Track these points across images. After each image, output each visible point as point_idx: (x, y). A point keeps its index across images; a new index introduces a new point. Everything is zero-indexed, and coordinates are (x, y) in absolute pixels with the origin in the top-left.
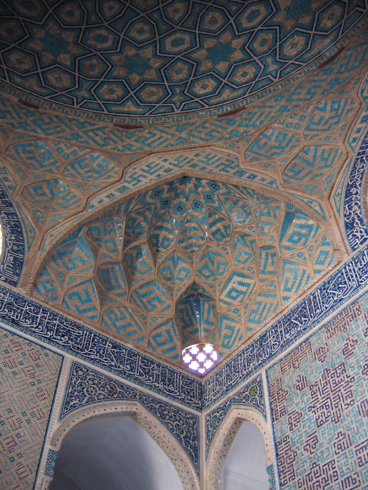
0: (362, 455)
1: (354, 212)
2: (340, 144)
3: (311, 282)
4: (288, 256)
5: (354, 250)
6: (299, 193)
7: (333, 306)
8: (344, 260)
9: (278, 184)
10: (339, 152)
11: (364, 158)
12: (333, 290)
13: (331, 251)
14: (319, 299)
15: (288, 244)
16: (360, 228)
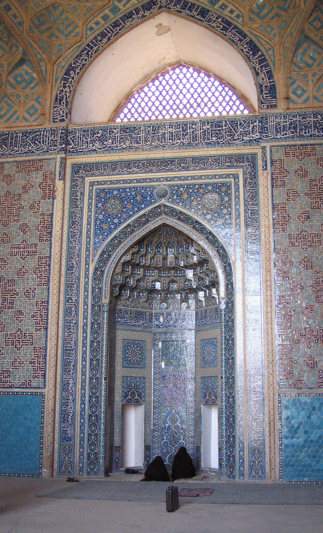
0: (13, 250)
1: (66, 92)
2: (80, 23)
3: (18, 124)
4: (9, 92)
5: (54, 122)
6: (36, 46)
7: (26, 153)
8: (46, 125)
9: (25, 28)
10: (77, 30)
11: (90, 53)
12: (30, 141)
13: (39, 111)
14: (19, 140)
15: (12, 81)
16: (64, 109)
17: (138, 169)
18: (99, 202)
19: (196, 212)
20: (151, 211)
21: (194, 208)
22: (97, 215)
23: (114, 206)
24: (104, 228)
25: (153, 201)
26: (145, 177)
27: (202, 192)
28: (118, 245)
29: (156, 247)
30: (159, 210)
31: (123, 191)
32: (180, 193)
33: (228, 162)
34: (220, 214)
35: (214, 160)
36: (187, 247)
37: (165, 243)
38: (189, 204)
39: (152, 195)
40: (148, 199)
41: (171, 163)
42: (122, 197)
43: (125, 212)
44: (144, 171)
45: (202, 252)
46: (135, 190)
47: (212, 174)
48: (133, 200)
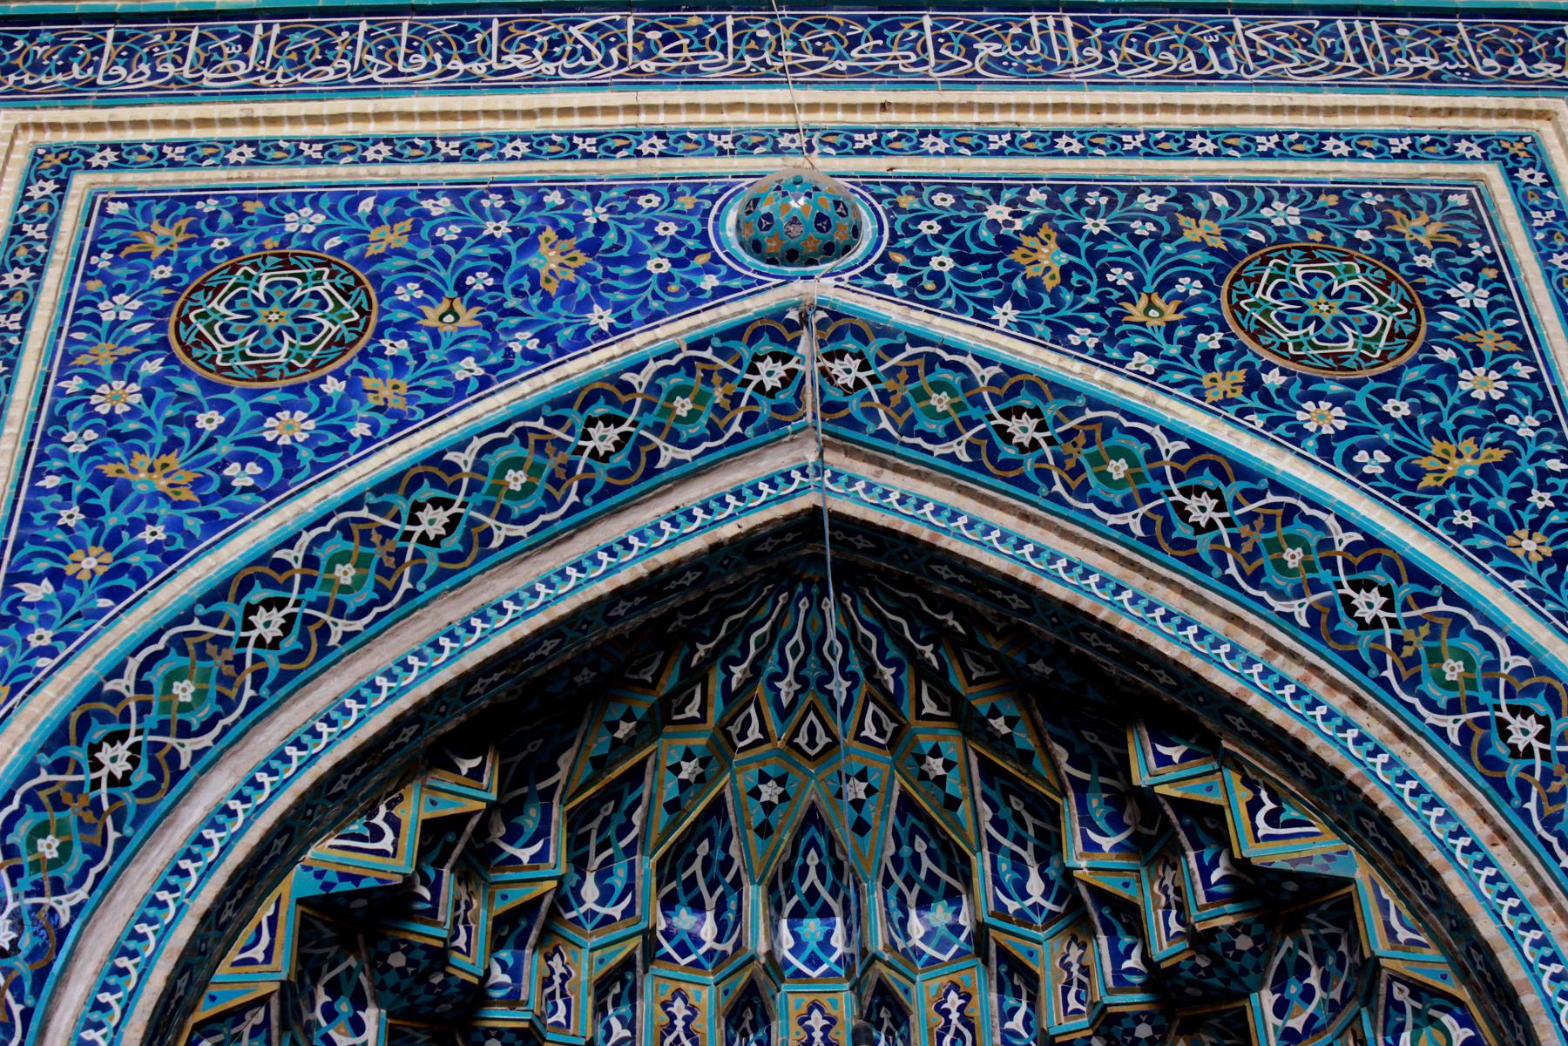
17: (549, 57)
18: (121, 289)
19: (1178, 377)
20: (684, 366)
21: (1152, 351)
22: (74, 385)
23: (274, 317)
24: (143, 482)
25: (709, 282)
26: (621, 121)
27: (1218, 243)
28: (284, 677)
29: (667, 869)
30: (771, 373)
31: (386, 210)
32: (985, 234)
33: (1420, 51)
34: (1434, 399)
35: (1285, 35)
36: (1008, 877)
37: (764, 830)
38: (1092, 317)
39: (691, 243)
40: (657, 264)
41: (877, 34)
42: (373, 250)
43: (399, 362)
44: (611, 71)
45: (1254, 806)
46: (515, 209)
47: (1285, 121)
48: (494, 273)
